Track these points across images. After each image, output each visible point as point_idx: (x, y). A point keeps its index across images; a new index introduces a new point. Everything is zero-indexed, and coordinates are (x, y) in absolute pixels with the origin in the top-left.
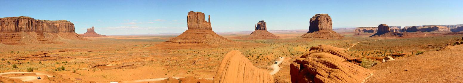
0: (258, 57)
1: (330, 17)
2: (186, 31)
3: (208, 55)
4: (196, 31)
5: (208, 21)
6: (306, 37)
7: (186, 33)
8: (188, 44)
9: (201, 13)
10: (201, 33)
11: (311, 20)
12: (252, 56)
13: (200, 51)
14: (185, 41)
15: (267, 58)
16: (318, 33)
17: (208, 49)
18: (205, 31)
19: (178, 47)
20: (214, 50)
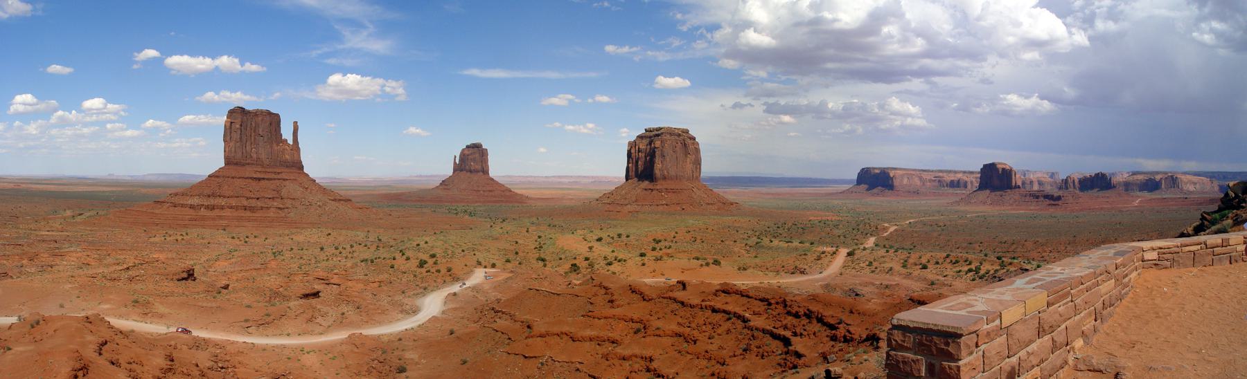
0: (422, 264)
1: (694, 139)
2: (218, 171)
3: (274, 253)
4: (249, 172)
5: (290, 142)
6: (613, 203)
7: (217, 177)
8: (222, 213)
9: (269, 113)
10: (268, 179)
11: (632, 145)
12: (404, 257)
13: (251, 240)
14: (212, 201)
15: (449, 270)
16: (652, 190)
17: (281, 232)
18: (279, 173)
19: (187, 222)
20: (300, 238)
